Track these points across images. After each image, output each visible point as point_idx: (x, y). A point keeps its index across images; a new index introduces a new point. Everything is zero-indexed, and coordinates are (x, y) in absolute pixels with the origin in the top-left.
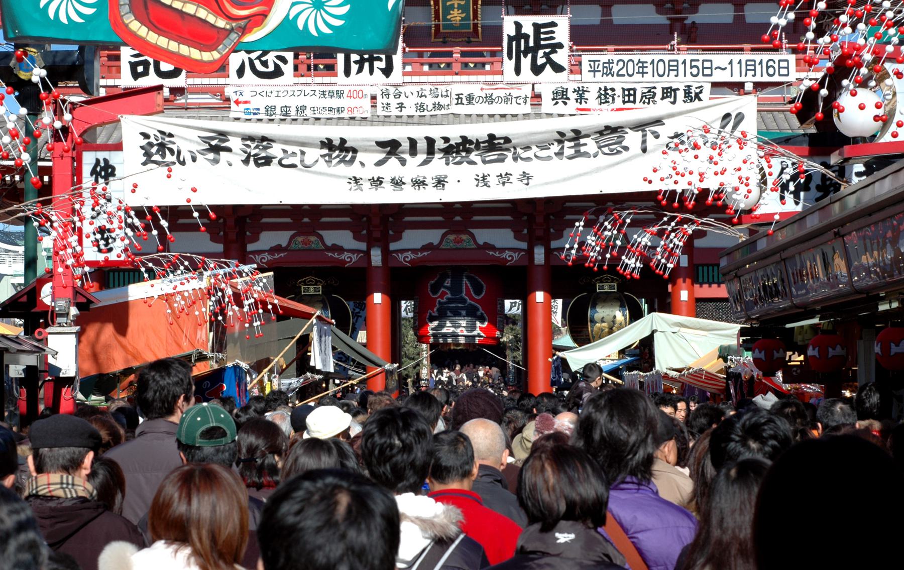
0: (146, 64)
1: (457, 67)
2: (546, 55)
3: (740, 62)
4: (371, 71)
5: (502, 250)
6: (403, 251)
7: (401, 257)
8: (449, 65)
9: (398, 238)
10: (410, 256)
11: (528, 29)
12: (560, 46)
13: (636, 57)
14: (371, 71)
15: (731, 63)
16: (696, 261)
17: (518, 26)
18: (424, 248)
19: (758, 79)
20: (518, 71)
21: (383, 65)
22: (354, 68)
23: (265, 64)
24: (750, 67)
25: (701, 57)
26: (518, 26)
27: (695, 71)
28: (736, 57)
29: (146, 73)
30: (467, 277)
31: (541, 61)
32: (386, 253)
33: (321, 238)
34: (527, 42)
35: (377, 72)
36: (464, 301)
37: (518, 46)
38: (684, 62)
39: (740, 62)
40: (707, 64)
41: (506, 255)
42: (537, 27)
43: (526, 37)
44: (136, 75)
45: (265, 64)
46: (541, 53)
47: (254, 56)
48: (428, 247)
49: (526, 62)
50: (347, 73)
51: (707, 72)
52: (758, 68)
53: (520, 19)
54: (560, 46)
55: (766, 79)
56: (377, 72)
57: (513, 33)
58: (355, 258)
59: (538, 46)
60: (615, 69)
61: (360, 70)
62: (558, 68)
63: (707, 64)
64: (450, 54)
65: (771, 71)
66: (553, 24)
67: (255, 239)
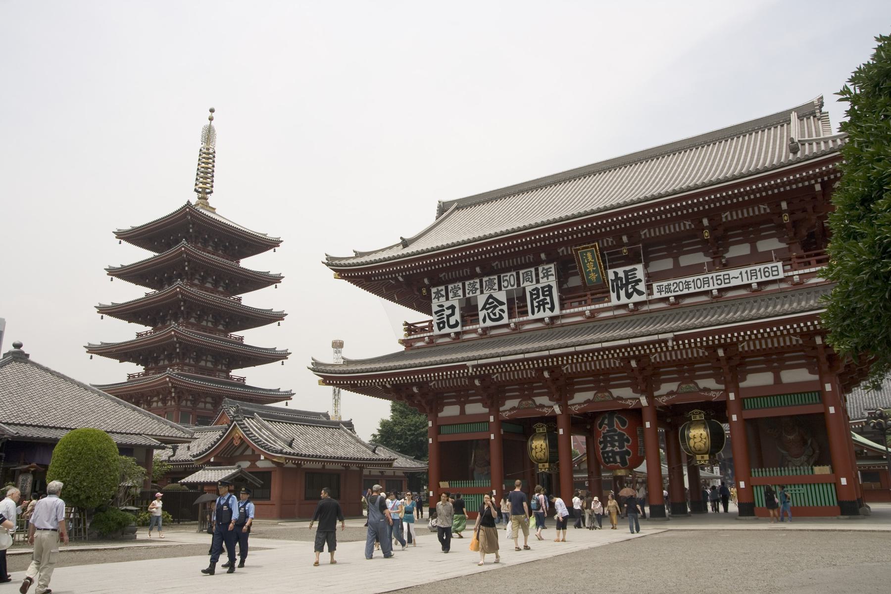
0: (443, 322)
1: (589, 301)
2: (633, 287)
3: (746, 272)
4: (544, 311)
5: (626, 400)
6: (574, 405)
7: (573, 408)
8: (585, 301)
9: (572, 398)
10: (578, 407)
11: (621, 274)
12: (640, 280)
13: (683, 280)
14: (544, 311)
15: (741, 273)
16: (741, 396)
17: (616, 274)
18: (585, 402)
19: (759, 280)
20: (619, 298)
21: (549, 306)
22: (536, 309)
23: (494, 314)
24: (754, 274)
25: (722, 273)
26: (616, 274)
27: (719, 282)
28: (744, 270)
29: (444, 327)
30: (618, 418)
31: (630, 291)
32: (564, 406)
33: (534, 401)
34: (622, 281)
35: (547, 310)
36: (616, 431)
37: (617, 285)
38: (712, 278)
39: (746, 272)
40: (726, 277)
41: (629, 402)
42: (624, 271)
43: (621, 279)
44: (440, 329)
45: (494, 314)
46: (630, 286)
47: (489, 311)
48: (588, 401)
49: (622, 293)
50: (533, 313)
51: (727, 281)
52: (759, 274)
53: (616, 270)
54: (640, 280)
55: (764, 279)
56: (547, 310)
57: (613, 278)
58: (550, 410)
59: (628, 283)
60: (672, 288)
61: (539, 311)
62: (640, 293)
63: (726, 277)
64: (585, 296)
65: (767, 274)
66: (635, 269)
67: (503, 404)
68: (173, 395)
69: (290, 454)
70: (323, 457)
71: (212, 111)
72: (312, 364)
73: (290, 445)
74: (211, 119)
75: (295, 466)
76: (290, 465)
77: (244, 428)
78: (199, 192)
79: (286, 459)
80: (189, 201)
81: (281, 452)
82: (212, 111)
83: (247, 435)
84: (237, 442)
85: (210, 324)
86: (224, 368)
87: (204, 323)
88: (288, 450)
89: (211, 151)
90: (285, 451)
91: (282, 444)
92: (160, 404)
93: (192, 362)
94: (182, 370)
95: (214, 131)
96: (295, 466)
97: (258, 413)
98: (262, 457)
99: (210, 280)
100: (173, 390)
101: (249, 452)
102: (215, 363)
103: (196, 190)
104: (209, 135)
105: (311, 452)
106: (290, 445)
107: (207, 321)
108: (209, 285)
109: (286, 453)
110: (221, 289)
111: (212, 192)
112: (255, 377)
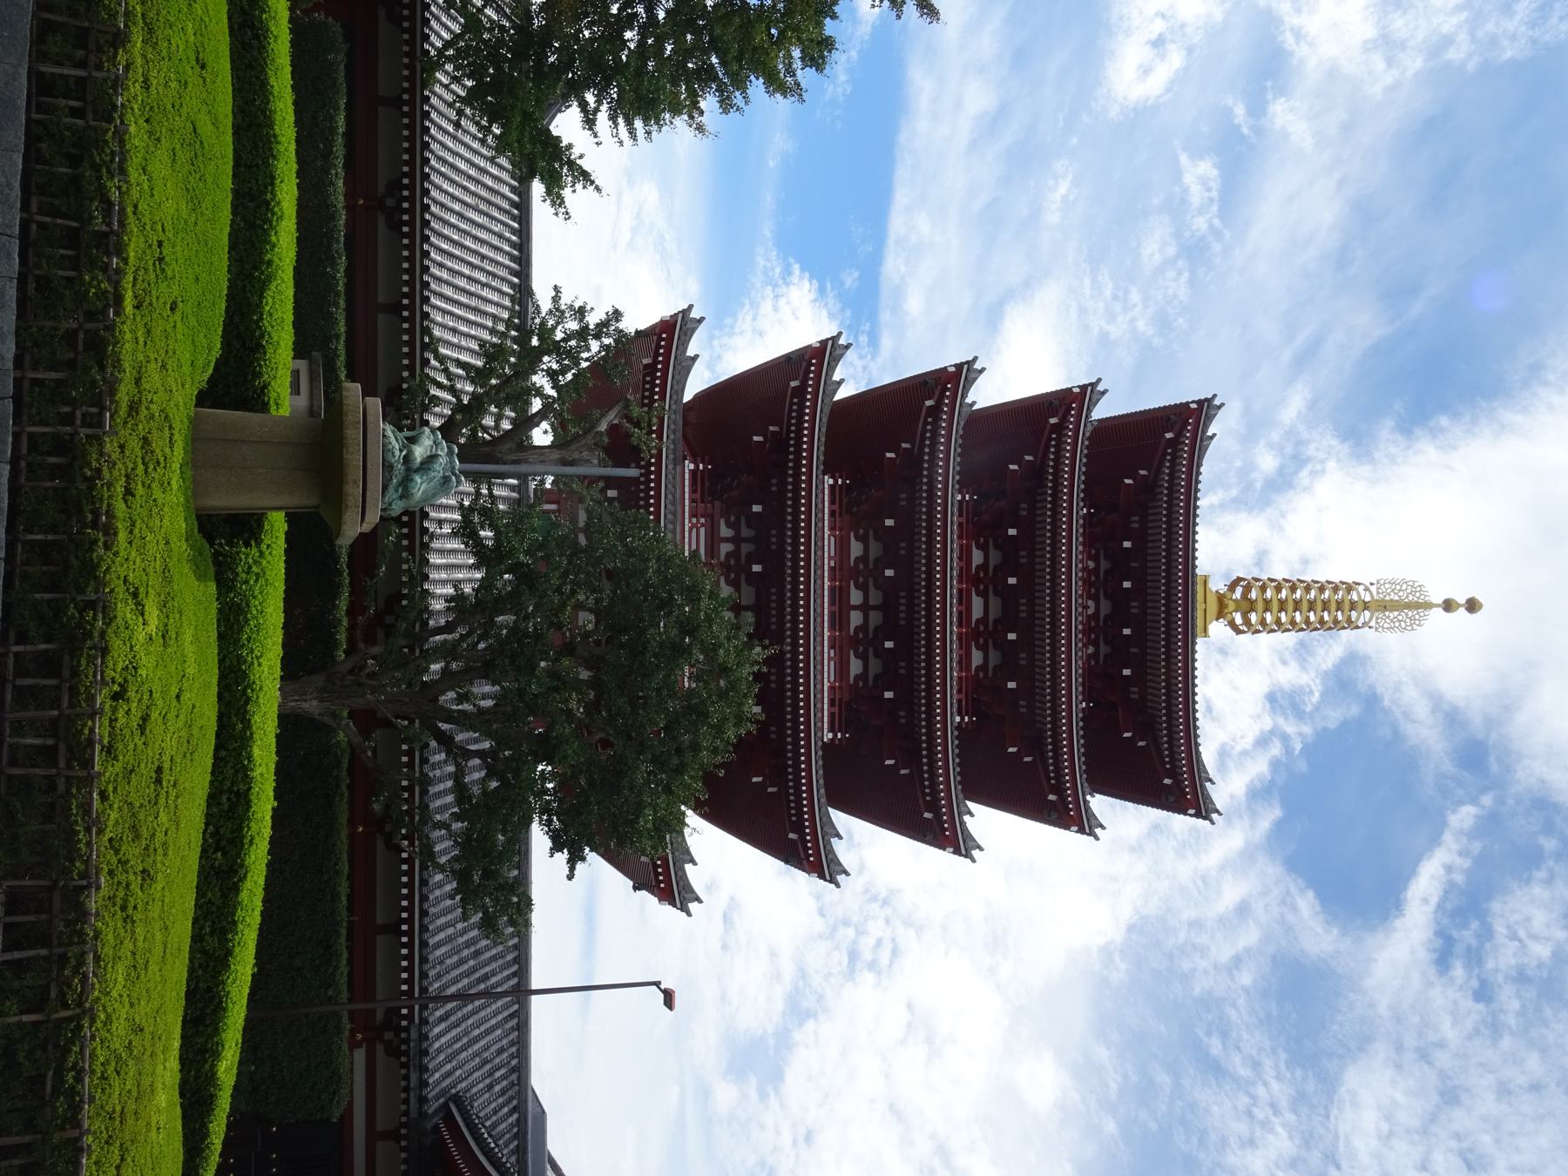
71: (1472, 606)
74: (1448, 606)
82: (1472, 606)
85: (856, 618)
87: (856, 597)
93: (725, 548)
107: (865, 608)
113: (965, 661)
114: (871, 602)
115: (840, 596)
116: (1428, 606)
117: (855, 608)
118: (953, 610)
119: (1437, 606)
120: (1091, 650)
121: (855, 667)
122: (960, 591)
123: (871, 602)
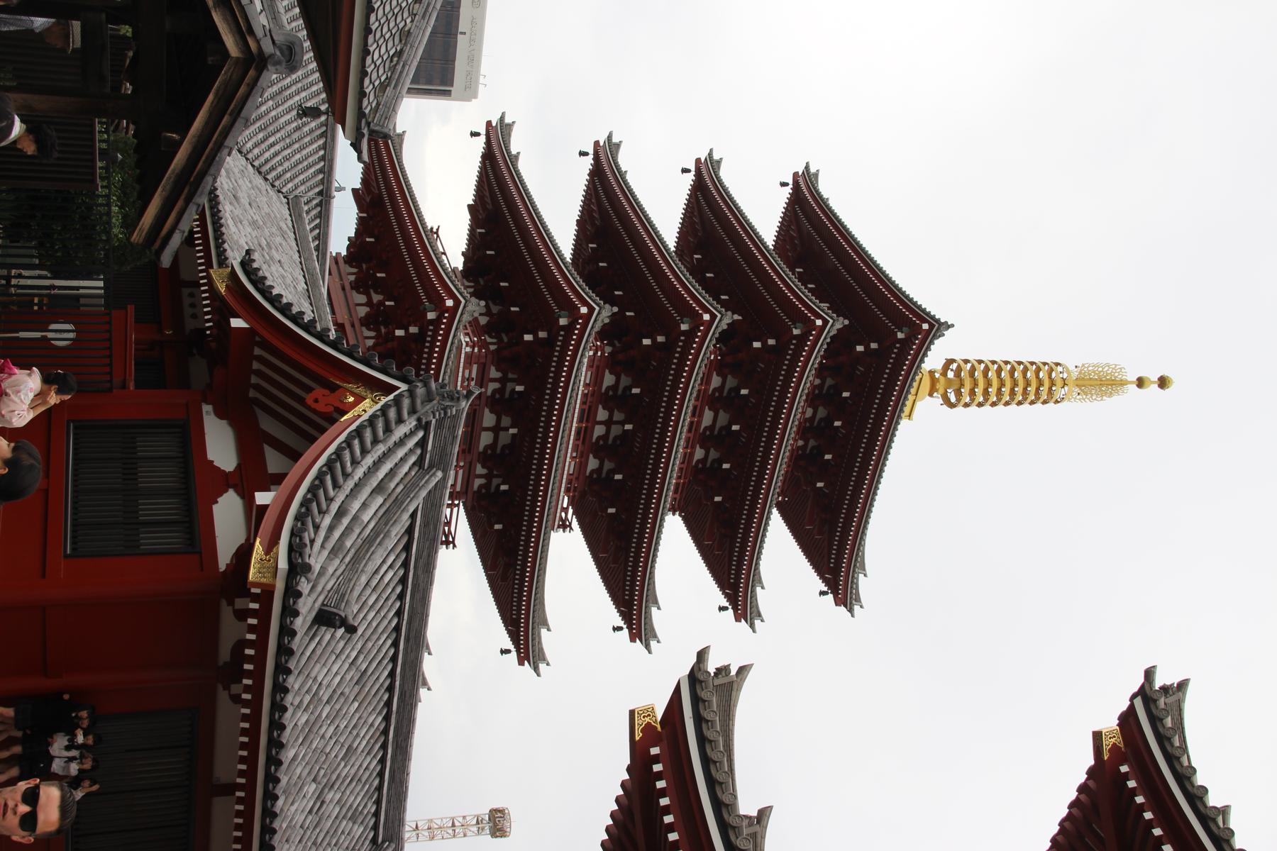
68: (400, 333)
69: (290, 612)
70: (272, 779)
71: (1163, 382)
72: (722, 671)
73: (325, 618)
74: (1141, 383)
75: (225, 654)
76: (231, 630)
77: (382, 422)
78: (944, 373)
79: (268, 593)
80: (949, 326)
81: (298, 568)
82: (1163, 382)
83: (359, 432)
84: (319, 398)
85: (599, 431)
86: (478, 482)
87: (602, 414)
88: (307, 607)
89: (1059, 392)
90: (304, 586)
91: (328, 583)
92: (363, 311)
94: (469, 357)
95: (1102, 394)
96: (225, 654)
97: (442, 484)
98: (262, 498)
99: (723, 418)
100: (413, 330)
101: (274, 461)
102: (489, 457)
103: (950, 362)
104: (1100, 383)
105: (295, 719)
106: (325, 618)
107: (608, 423)
108: (708, 417)
109: (292, 593)
110: (699, 453)
111: (952, 406)
112: (460, 572)
113: (688, 457)
114: (615, 419)
115: (588, 416)
116: (1123, 383)
117: (600, 423)
118: (686, 418)
119: (1131, 383)
120: (800, 443)
121: (593, 463)
122: (695, 408)
123: (615, 419)
